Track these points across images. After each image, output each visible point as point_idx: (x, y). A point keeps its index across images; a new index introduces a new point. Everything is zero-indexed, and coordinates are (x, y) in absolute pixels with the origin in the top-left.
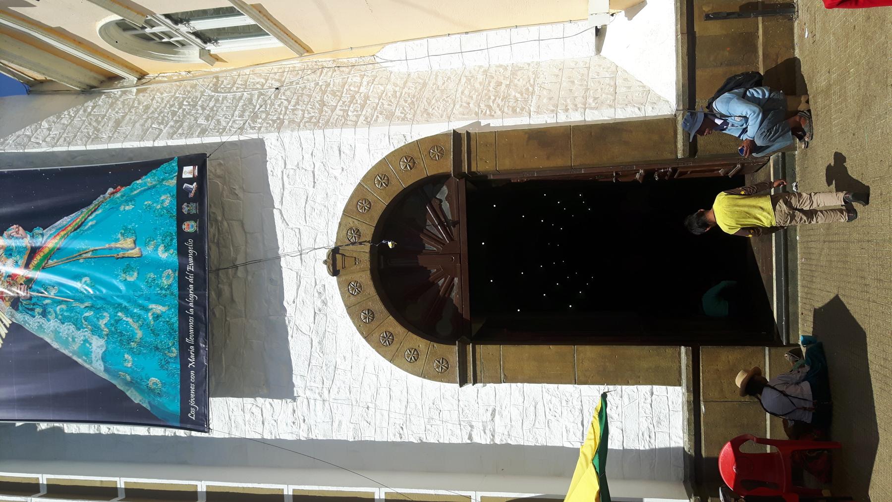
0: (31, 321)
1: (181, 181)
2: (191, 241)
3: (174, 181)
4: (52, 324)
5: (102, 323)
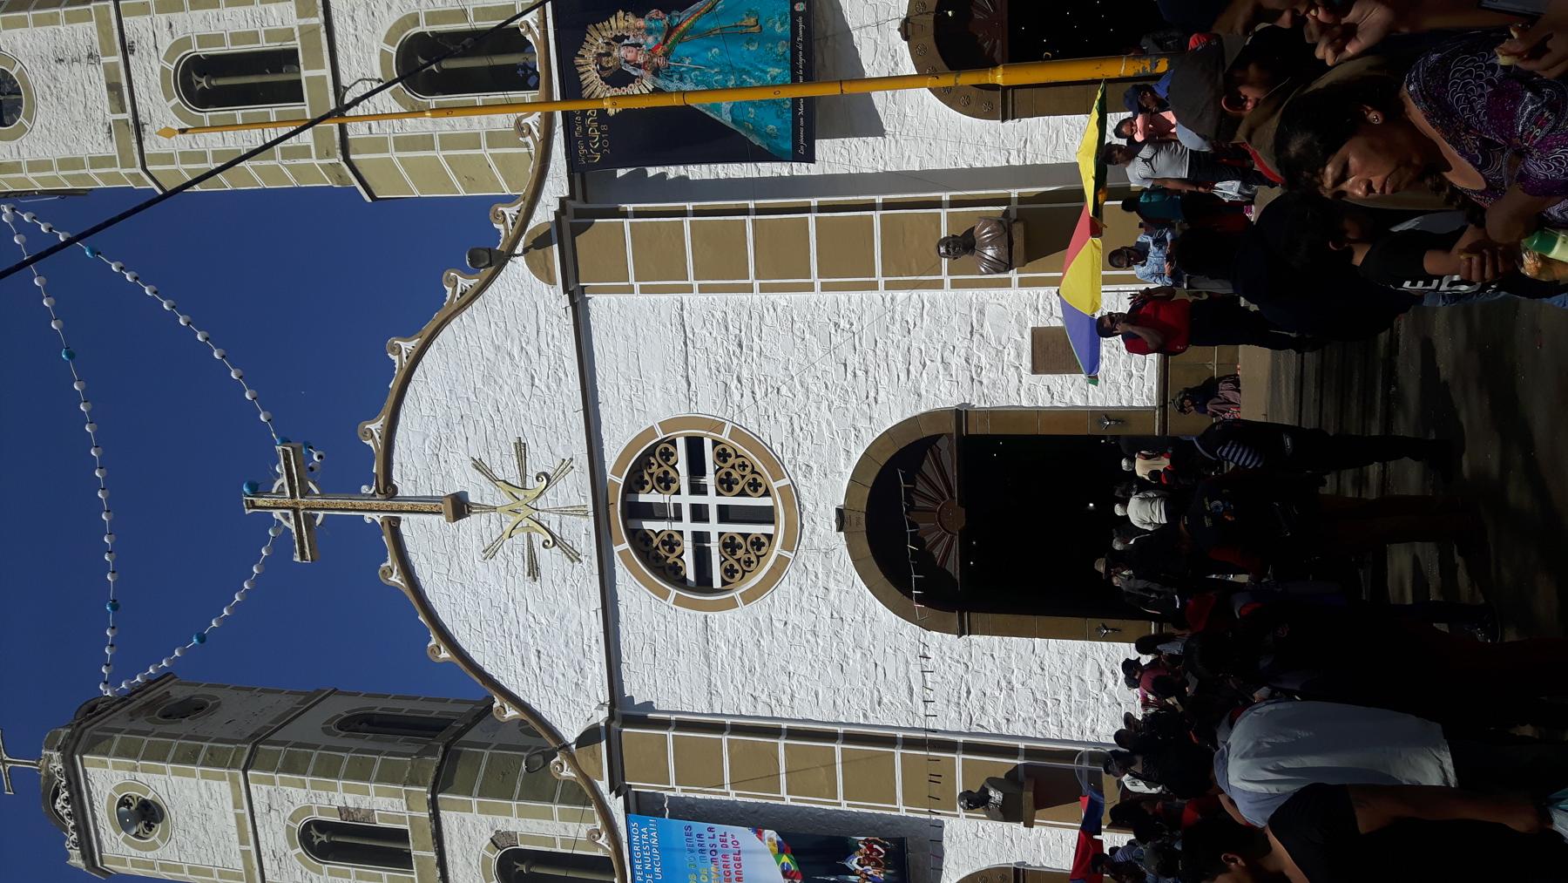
0: (671, 85)
2: (801, 18)
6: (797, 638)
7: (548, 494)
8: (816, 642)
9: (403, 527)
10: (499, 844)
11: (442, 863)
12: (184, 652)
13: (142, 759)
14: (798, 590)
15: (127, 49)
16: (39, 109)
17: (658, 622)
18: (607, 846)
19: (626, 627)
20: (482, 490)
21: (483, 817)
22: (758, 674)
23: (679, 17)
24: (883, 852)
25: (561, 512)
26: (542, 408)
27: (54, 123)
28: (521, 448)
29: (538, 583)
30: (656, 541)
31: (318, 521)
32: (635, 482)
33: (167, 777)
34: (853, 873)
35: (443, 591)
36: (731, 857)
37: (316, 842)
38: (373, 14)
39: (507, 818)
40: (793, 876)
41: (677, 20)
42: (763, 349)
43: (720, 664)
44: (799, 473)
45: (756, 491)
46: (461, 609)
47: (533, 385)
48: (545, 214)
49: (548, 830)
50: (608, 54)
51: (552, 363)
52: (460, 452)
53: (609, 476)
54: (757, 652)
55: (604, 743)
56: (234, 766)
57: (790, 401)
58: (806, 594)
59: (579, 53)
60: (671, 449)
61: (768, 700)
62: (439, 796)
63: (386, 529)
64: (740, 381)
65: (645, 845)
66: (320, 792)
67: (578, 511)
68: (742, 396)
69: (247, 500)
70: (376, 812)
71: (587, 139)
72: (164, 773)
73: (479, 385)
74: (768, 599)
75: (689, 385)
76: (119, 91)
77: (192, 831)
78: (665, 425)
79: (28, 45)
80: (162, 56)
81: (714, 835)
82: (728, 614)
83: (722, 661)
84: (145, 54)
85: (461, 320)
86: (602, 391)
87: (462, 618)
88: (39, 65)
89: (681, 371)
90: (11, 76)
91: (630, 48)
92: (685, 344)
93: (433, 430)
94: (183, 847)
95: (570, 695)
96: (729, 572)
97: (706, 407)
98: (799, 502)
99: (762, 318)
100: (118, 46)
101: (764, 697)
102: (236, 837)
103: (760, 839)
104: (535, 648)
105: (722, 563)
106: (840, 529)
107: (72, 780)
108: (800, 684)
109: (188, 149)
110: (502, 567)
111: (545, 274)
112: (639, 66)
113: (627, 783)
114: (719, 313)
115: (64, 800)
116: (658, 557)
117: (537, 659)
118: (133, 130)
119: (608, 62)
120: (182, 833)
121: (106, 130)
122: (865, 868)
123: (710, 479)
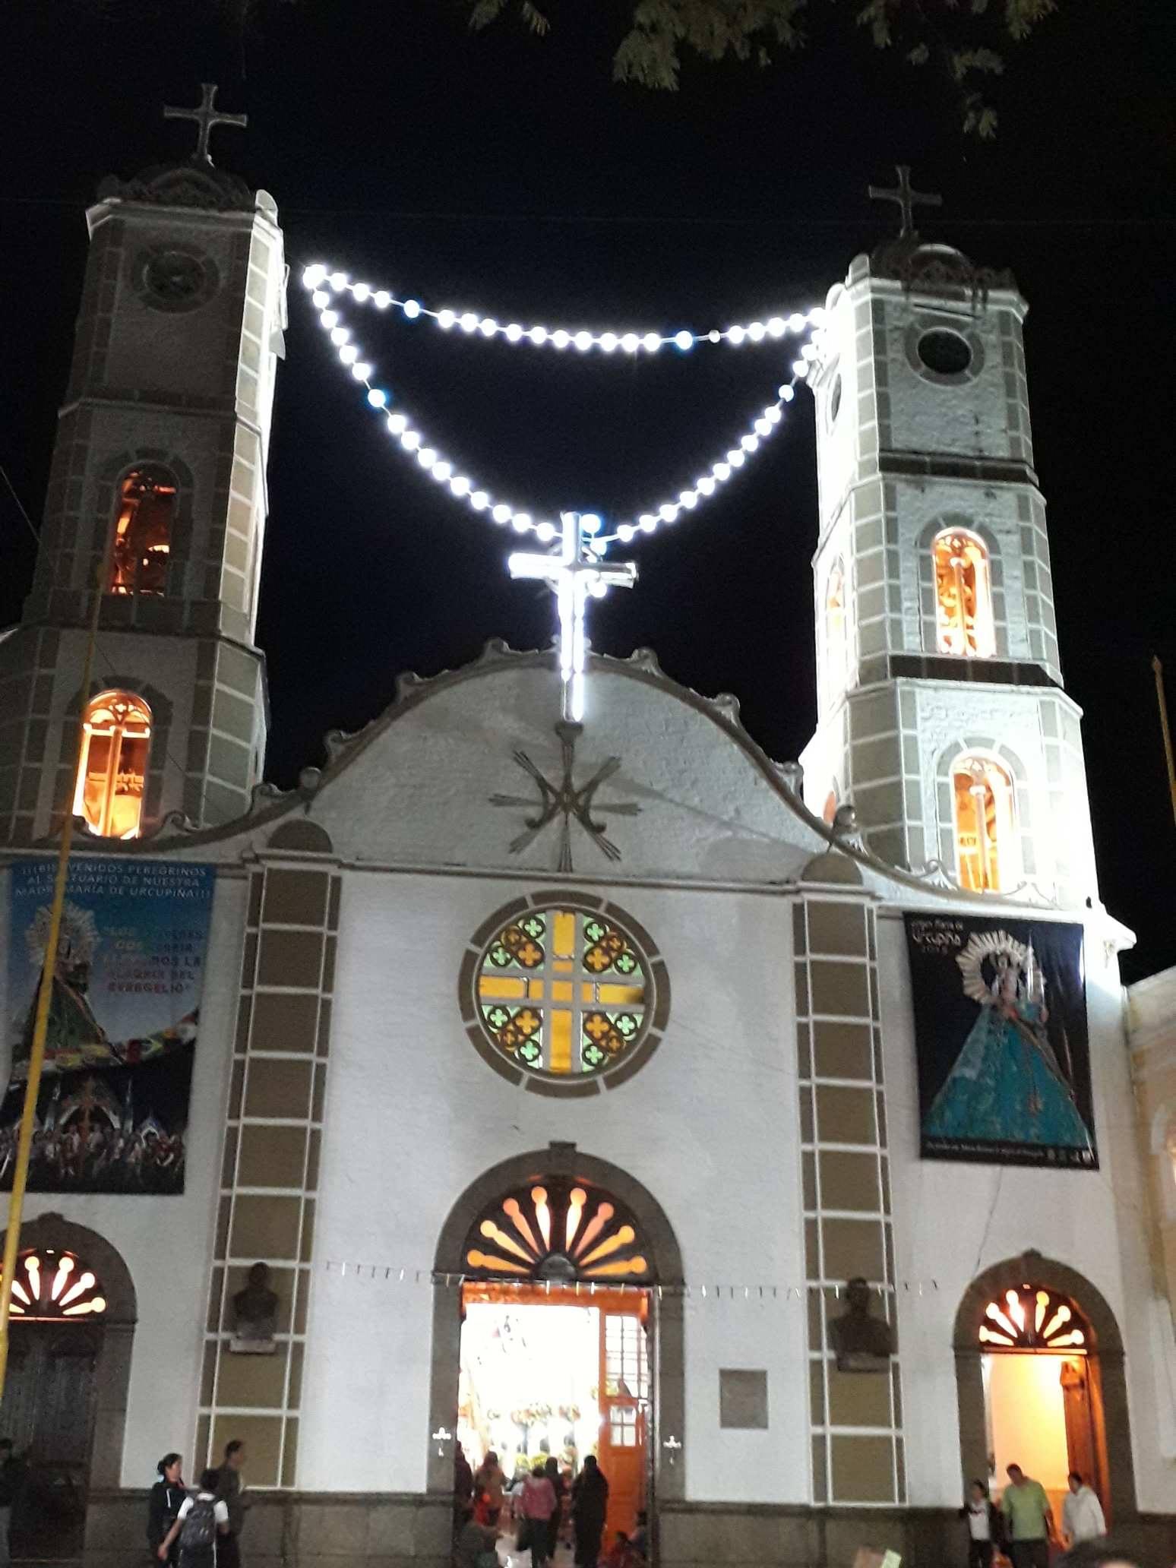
4: (983, 1036)
7: (586, 835)
24: (165, 1164)
34: (137, 1126)
67: (565, 862)
106: (553, 1144)
122: (144, 1141)
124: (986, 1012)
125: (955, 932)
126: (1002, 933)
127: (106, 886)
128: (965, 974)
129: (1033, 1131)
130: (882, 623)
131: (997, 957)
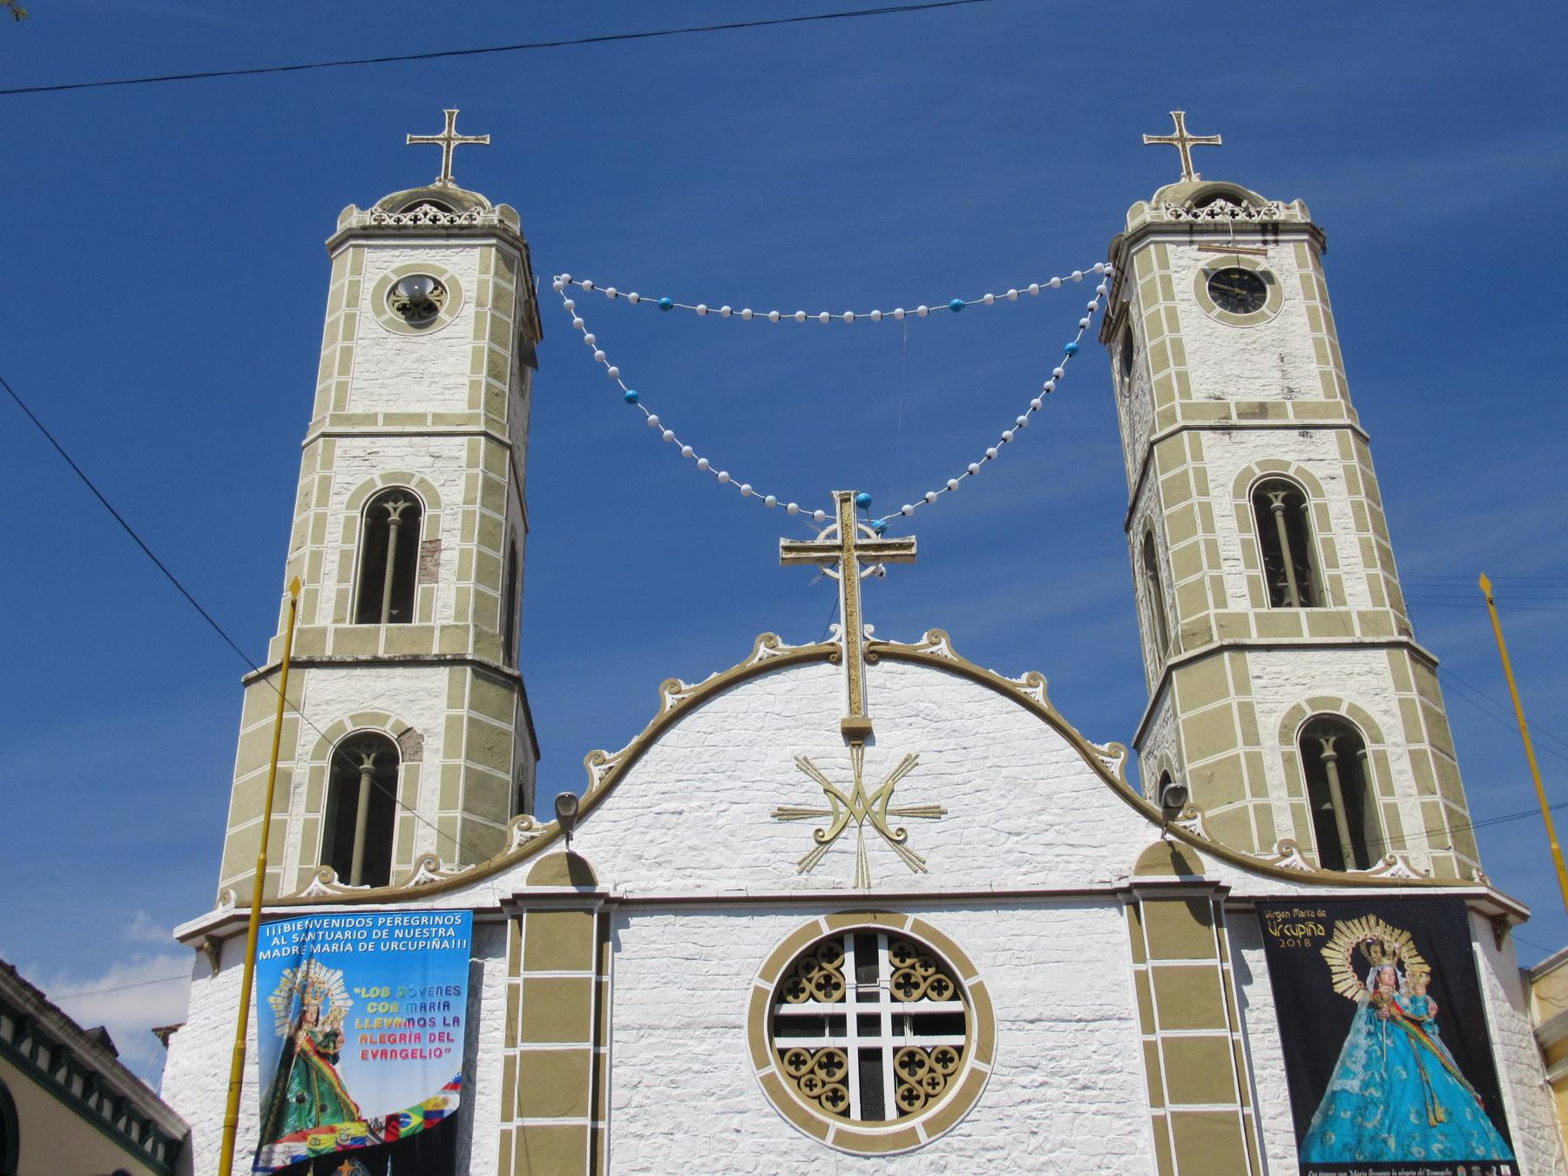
1: (1498, 1164)
2: (1450, 1173)
3: (1496, 1158)
4: (1363, 1042)
5: (1372, 1090)
6: (720, 1146)
7: (881, 841)
8: (717, 1171)
9: (826, 668)
10: (404, 738)
11: (376, 663)
12: (614, 378)
13: (492, 315)
14: (785, 1150)
15: (1304, 429)
16: (1230, 329)
17: (731, 965)
18: (416, 879)
19: (722, 925)
20: (880, 763)
21: (442, 721)
22: (669, 1091)
23: (1434, 1033)
25: (860, 855)
26: (984, 842)
27: (1218, 341)
28: (934, 813)
29: (770, 819)
30: (829, 968)
31: (828, 571)
32: (903, 946)
33: (471, 339)
35: (752, 705)
36: (418, 1046)
37: (390, 506)
38: (1377, 694)
39: (442, 750)
40: (390, 1128)
41: (1430, 1031)
42: (1083, 1116)
43: (679, 1042)
44: (934, 1157)
45: (904, 1098)
46: (730, 724)
47: (1010, 833)
48: (1212, 870)
49: (426, 801)
50: (1384, 953)
51: (1038, 859)
52: (924, 743)
53: (912, 917)
54: (697, 1091)
55: (572, 890)
56: (488, 421)
57: (1023, 1147)
58: (780, 1160)
59: (1381, 921)
60: (948, 994)
61: (634, 1104)
62: (469, 669)
63: (823, 647)
64: (1042, 1084)
65: (430, 932)
66: (460, 520)
68: (1024, 1087)
69: (850, 494)
70: (435, 585)
71: (1294, 921)
72: (476, 337)
73: (1004, 772)
74: (768, 1109)
75: (1032, 1022)
76: (1259, 415)
77: (400, 359)
78: (980, 989)
79: (1293, 328)
80: (1302, 464)
81: (449, 1025)
82: (746, 1056)
83: (684, 1045)
84: (1301, 448)
85: (1077, 760)
86: (1013, 916)
87: (720, 724)
88: (1276, 336)
89: (1048, 1013)
90: (1260, 306)
91: (1393, 978)
92: (1080, 1021)
93: (948, 714)
94: (379, 345)
95: (626, 847)
96: (797, 1060)
97: (1004, 1040)
98: (898, 1154)
99: (1119, 1116)
100: (1307, 422)
101: (638, 1098)
102: (394, 410)
103: (446, 1088)
104: (686, 809)
105: (807, 1050)
107: (465, 232)
108: (659, 1148)
109: (1210, 477)
110: (788, 778)
111: (1147, 862)
112: (1376, 987)
113: (525, 915)
114: (1120, 1063)
115: (435, 217)
116: (809, 969)
117: (672, 810)
118: (1223, 423)
119: (1376, 952)
120: (397, 346)
121: (1217, 394)
123: (911, 1040)
124: (1362, 1011)
125: (1317, 921)
126: (1372, 919)
127: (355, 942)
128: (1334, 969)
129: (1436, 1147)
130: (1201, 581)
131: (1368, 946)
